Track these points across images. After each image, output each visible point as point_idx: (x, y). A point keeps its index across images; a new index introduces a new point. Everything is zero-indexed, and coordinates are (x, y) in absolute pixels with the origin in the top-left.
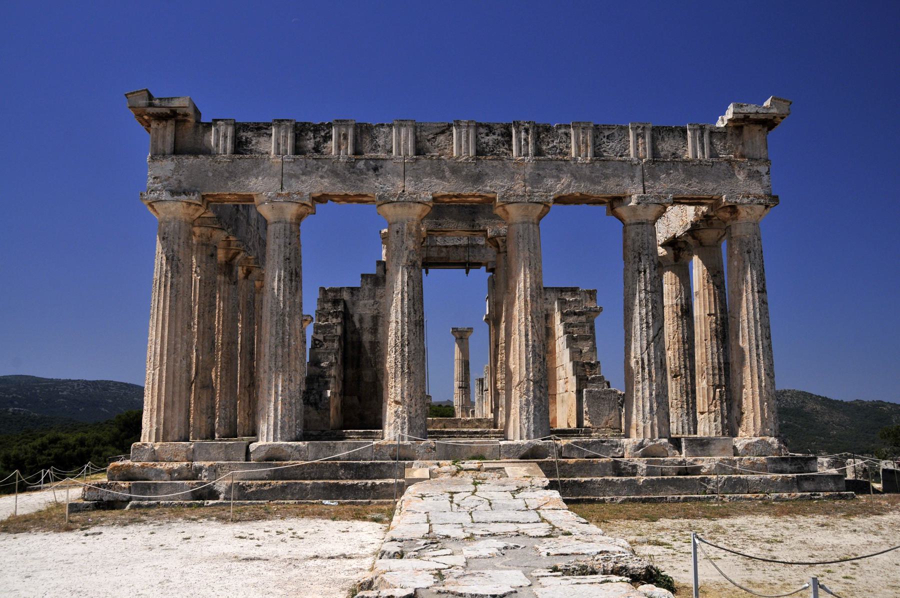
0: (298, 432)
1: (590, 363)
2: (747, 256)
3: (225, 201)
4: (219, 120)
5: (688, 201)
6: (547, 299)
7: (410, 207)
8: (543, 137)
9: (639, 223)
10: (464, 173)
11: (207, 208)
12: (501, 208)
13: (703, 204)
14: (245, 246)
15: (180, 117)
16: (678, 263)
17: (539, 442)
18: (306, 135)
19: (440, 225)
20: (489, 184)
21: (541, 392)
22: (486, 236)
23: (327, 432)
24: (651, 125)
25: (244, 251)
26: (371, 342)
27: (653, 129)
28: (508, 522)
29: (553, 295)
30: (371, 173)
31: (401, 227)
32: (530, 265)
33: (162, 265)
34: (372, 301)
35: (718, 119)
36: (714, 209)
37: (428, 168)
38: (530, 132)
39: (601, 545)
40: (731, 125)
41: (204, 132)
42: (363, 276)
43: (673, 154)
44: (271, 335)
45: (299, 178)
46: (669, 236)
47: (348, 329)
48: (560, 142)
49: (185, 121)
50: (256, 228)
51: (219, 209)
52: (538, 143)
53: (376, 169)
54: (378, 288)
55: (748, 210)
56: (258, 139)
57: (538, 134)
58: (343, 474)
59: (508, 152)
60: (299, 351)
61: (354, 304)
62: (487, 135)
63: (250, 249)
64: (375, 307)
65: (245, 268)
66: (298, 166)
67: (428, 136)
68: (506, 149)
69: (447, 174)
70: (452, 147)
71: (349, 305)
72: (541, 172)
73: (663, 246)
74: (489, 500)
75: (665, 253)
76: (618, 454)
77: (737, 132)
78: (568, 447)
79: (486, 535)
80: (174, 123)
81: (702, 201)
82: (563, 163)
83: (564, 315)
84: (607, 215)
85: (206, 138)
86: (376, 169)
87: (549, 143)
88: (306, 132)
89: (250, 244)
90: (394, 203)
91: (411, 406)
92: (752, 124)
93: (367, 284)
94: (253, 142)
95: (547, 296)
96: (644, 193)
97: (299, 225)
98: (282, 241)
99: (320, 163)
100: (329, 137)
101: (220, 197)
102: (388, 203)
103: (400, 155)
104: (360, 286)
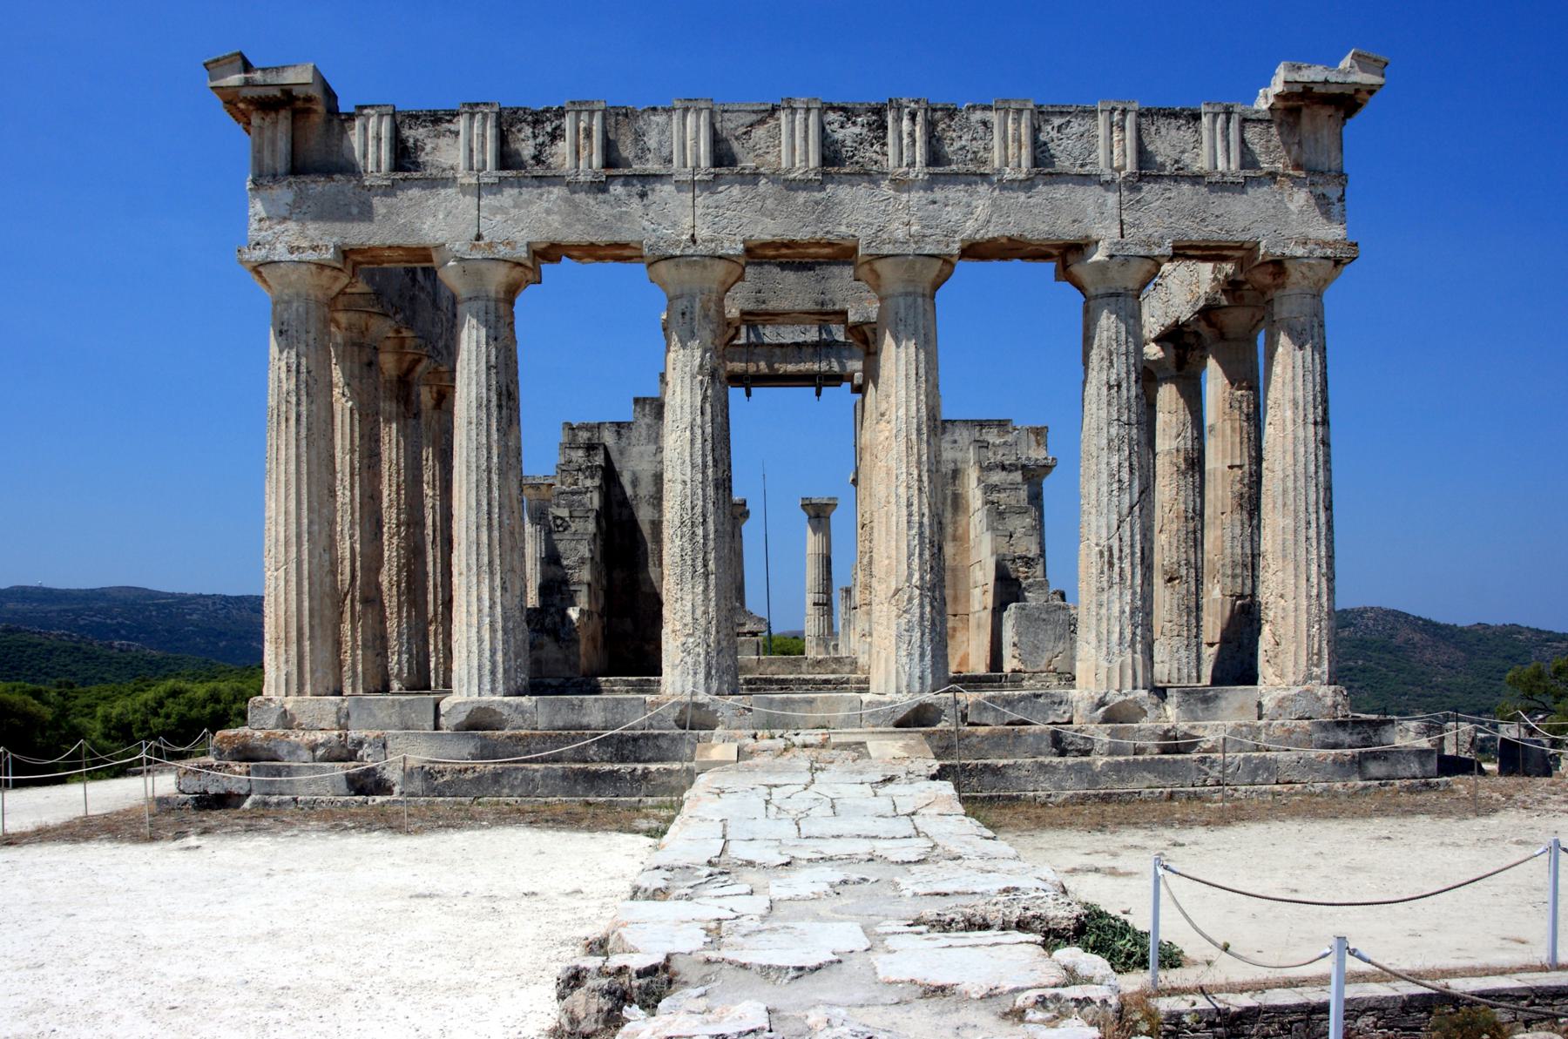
3: (383, 262)
5: (1198, 253)
6: (955, 442)
7: (705, 267)
9: (1112, 295)
11: (354, 275)
13: (1225, 259)
14: (430, 347)
16: (1183, 373)
19: (764, 302)
20: (845, 221)
22: (845, 321)
24: (1136, 106)
25: (429, 357)
27: (1140, 115)
29: (965, 434)
30: (635, 201)
35: (1257, 94)
36: (1246, 268)
40: (1280, 105)
42: (637, 401)
45: (507, 213)
46: (1169, 321)
50: (450, 315)
53: (643, 195)
55: (1304, 269)
63: (439, 353)
65: (435, 389)
69: (770, 203)
73: (1157, 340)
75: (1161, 354)
79: (817, 860)
81: (1225, 253)
84: (1057, 279)
86: (643, 195)
89: (441, 344)
96: (1122, 236)
97: (512, 304)
101: (374, 253)
102: (666, 259)
104: (631, 419)
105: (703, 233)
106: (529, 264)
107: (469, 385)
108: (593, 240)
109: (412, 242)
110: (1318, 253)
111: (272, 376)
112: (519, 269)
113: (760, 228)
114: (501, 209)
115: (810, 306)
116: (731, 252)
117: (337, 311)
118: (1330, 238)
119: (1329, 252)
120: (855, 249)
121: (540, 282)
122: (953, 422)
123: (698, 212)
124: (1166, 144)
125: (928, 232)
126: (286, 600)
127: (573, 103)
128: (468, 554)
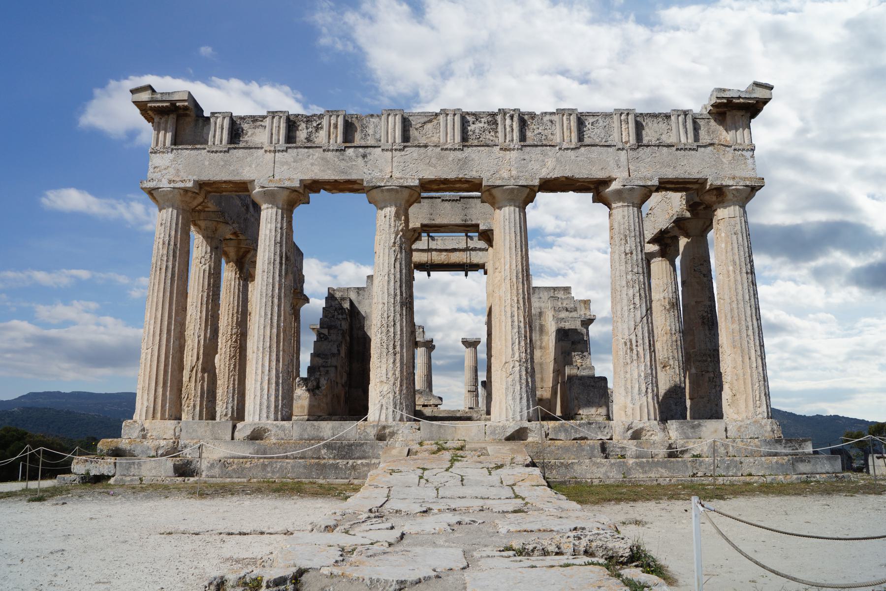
0: (284, 412)
2: (735, 237)
3: (223, 191)
4: (216, 113)
5: (673, 186)
6: (540, 298)
10: (450, 159)
12: (487, 193)
15: (181, 112)
17: (526, 424)
19: (434, 220)
20: (475, 169)
28: (477, 498)
29: (546, 294)
30: (360, 159)
33: (158, 249)
37: (415, 155)
39: (577, 521)
41: (204, 126)
43: (658, 139)
44: (260, 316)
45: (290, 165)
46: (656, 231)
48: (546, 129)
49: (186, 115)
51: (223, 204)
53: (364, 156)
55: (734, 192)
56: (254, 130)
58: (325, 454)
59: (494, 139)
60: (287, 332)
61: (359, 303)
62: (473, 124)
69: (433, 161)
71: (356, 304)
72: (526, 157)
74: (462, 476)
76: (606, 436)
77: (721, 118)
78: (554, 428)
80: (175, 116)
81: (688, 186)
83: (556, 310)
84: (593, 202)
85: (205, 131)
86: (364, 156)
92: (735, 109)
94: (249, 134)
95: (541, 295)
96: (630, 176)
98: (273, 226)
103: (387, 142)
104: (365, 286)
105: (396, 174)
106: (301, 191)
107: (264, 252)
108: (337, 178)
109: (237, 178)
110: (741, 183)
111: (155, 247)
112: (296, 193)
113: (428, 172)
114: (286, 163)
115: (458, 221)
116: (412, 184)
117: (200, 220)
118: (747, 176)
119: (748, 183)
120: (481, 184)
121: (309, 203)
122: (539, 288)
123: (394, 165)
124: (652, 131)
125: (521, 174)
126: (150, 365)
127: (328, 111)
128: (258, 341)
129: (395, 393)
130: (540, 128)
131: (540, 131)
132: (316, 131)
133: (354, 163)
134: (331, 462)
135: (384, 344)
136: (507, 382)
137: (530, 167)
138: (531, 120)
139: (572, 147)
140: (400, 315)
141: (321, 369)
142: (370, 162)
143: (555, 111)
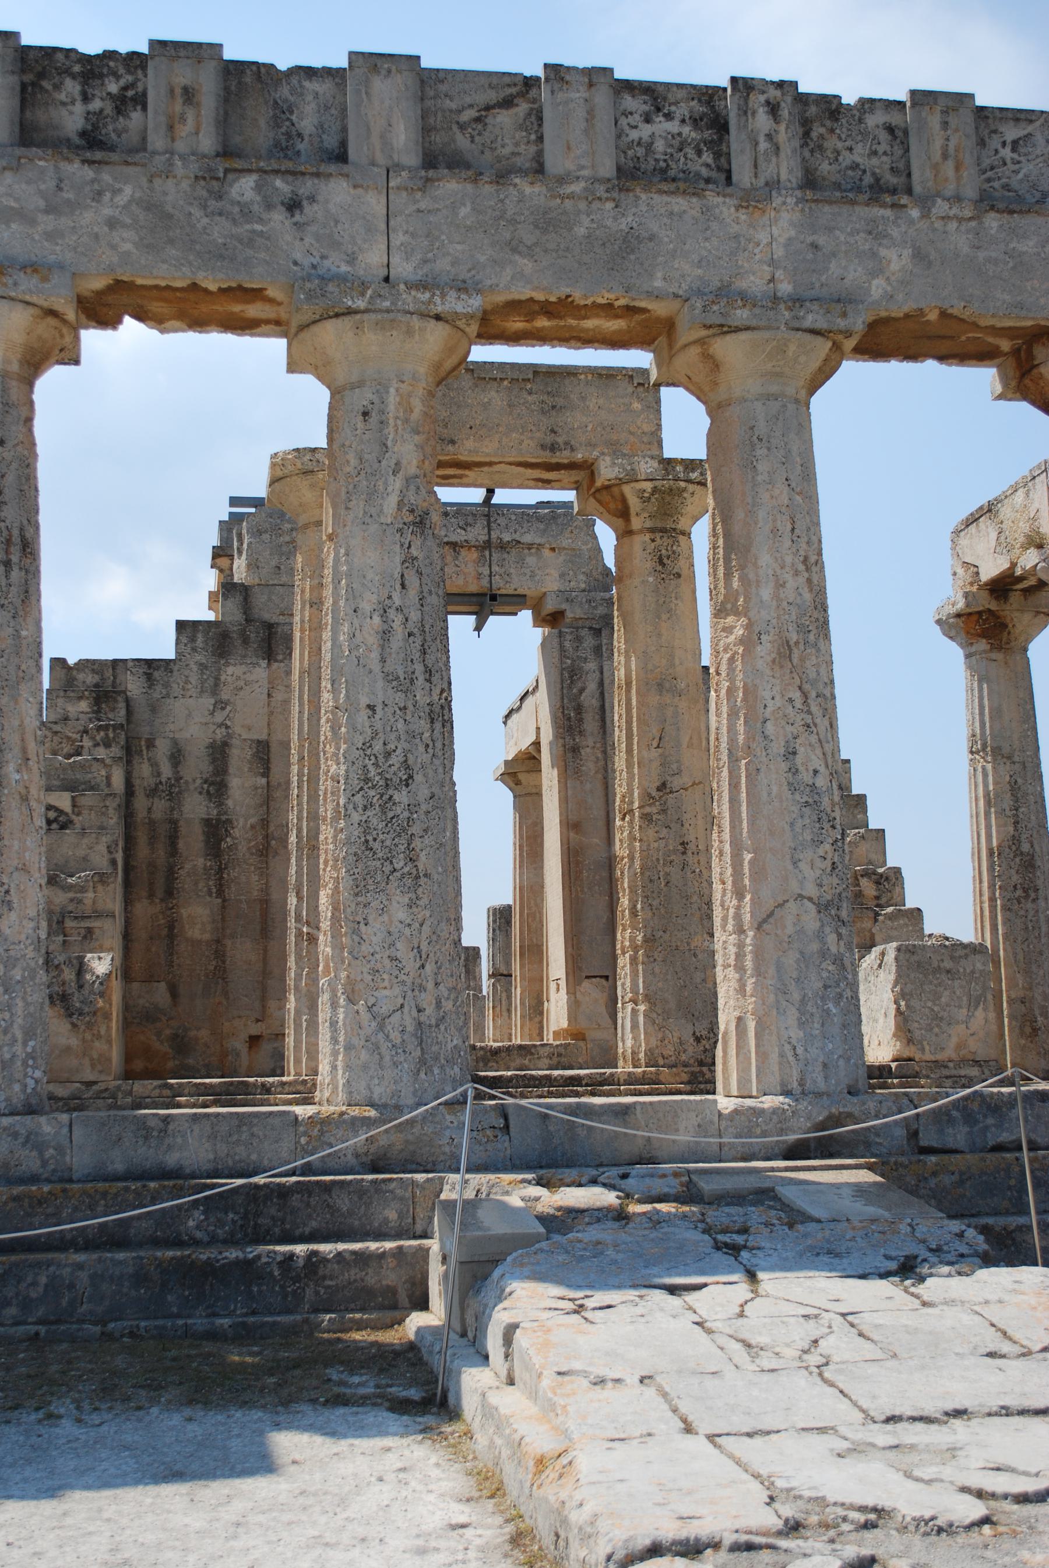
0: (31, 1083)
1: (875, 873)
7: (409, 332)
8: (821, 136)
10: (581, 231)
18: (57, 87)
19: (453, 442)
21: (840, 936)
23: (101, 1086)
26: (207, 822)
30: (278, 217)
31: (376, 401)
32: (793, 529)
34: (208, 702)
38: (785, 113)
45: (32, 222)
47: (137, 782)
48: (875, 153)
52: (807, 154)
53: (293, 206)
54: (227, 664)
57: (806, 125)
58: (198, 1227)
59: (714, 174)
61: (154, 709)
62: (648, 120)
64: (219, 717)
66: (29, 182)
67: (459, 112)
68: (708, 165)
70: (540, 153)
71: (142, 713)
72: (821, 240)
82: (888, 213)
86: (293, 206)
87: (838, 153)
88: (56, 80)
90: (358, 316)
91: (422, 988)
93: (194, 650)
99: (106, 177)
100: (132, 99)
102: (337, 315)
104: (171, 655)
112: (51, 321)
123: (399, 238)
129: (420, 1011)
130: (859, 149)
131: (859, 160)
132: (119, 111)
133: (258, 227)
134: (233, 1254)
135: (376, 846)
136: (779, 967)
137: (834, 268)
138: (828, 123)
139: (967, 213)
140: (427, 746)
141: (69, 923)
142: (313, 228)
143: (902, 96)
